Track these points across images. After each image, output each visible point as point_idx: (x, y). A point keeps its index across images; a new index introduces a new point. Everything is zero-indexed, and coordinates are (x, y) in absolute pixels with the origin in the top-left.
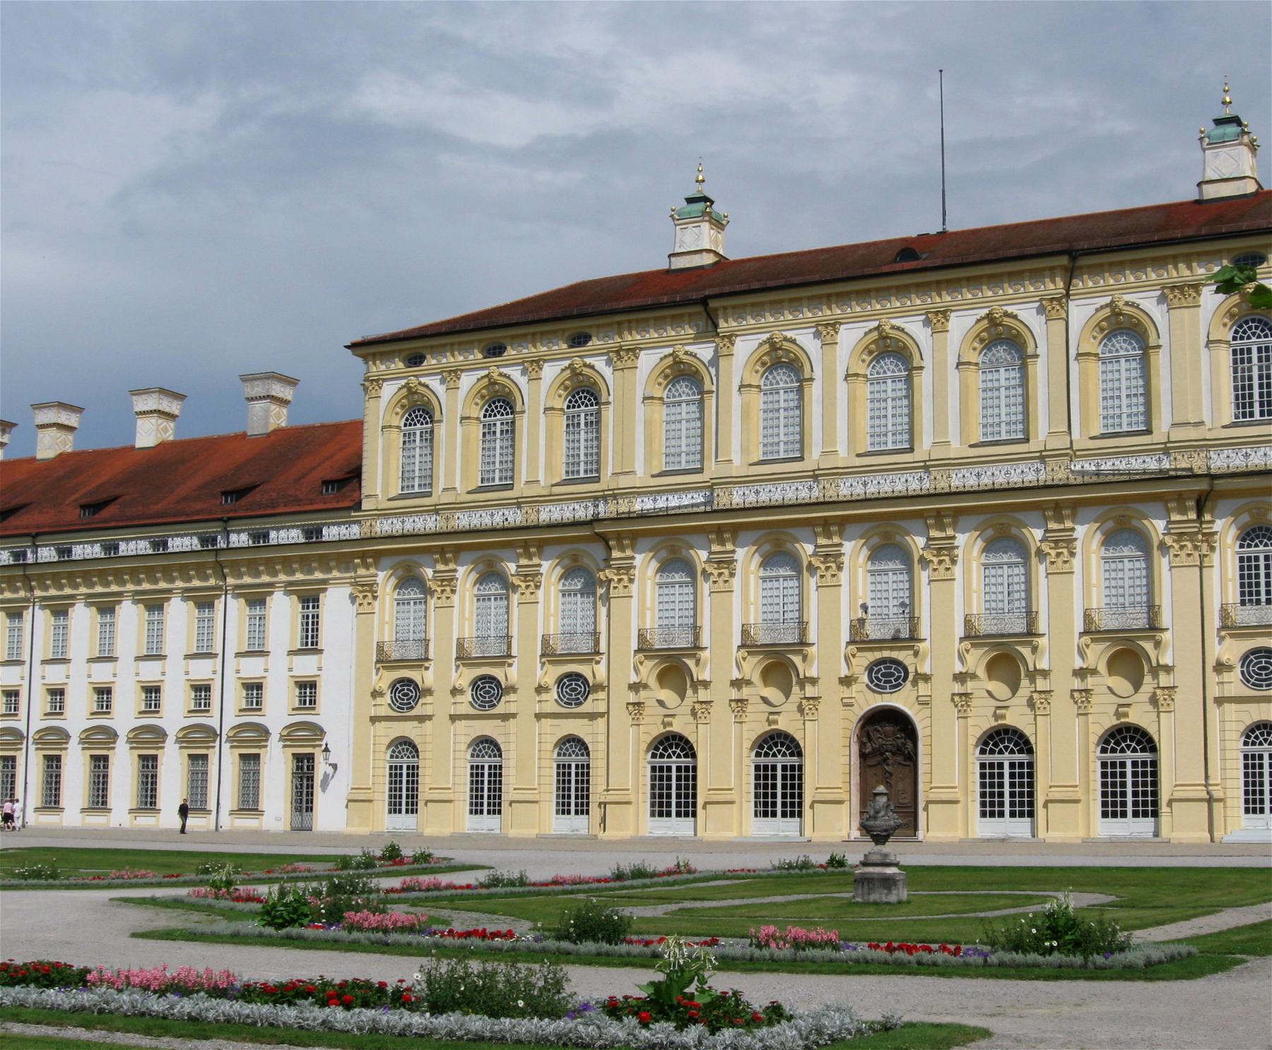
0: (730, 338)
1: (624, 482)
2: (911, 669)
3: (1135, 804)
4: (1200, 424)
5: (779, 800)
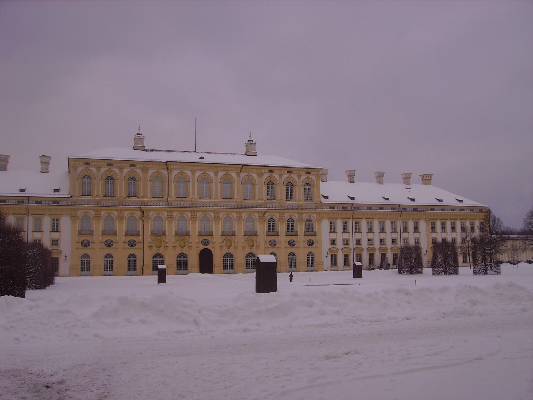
0: (172, 170)
1: (146, 199)
2: (211, 241)
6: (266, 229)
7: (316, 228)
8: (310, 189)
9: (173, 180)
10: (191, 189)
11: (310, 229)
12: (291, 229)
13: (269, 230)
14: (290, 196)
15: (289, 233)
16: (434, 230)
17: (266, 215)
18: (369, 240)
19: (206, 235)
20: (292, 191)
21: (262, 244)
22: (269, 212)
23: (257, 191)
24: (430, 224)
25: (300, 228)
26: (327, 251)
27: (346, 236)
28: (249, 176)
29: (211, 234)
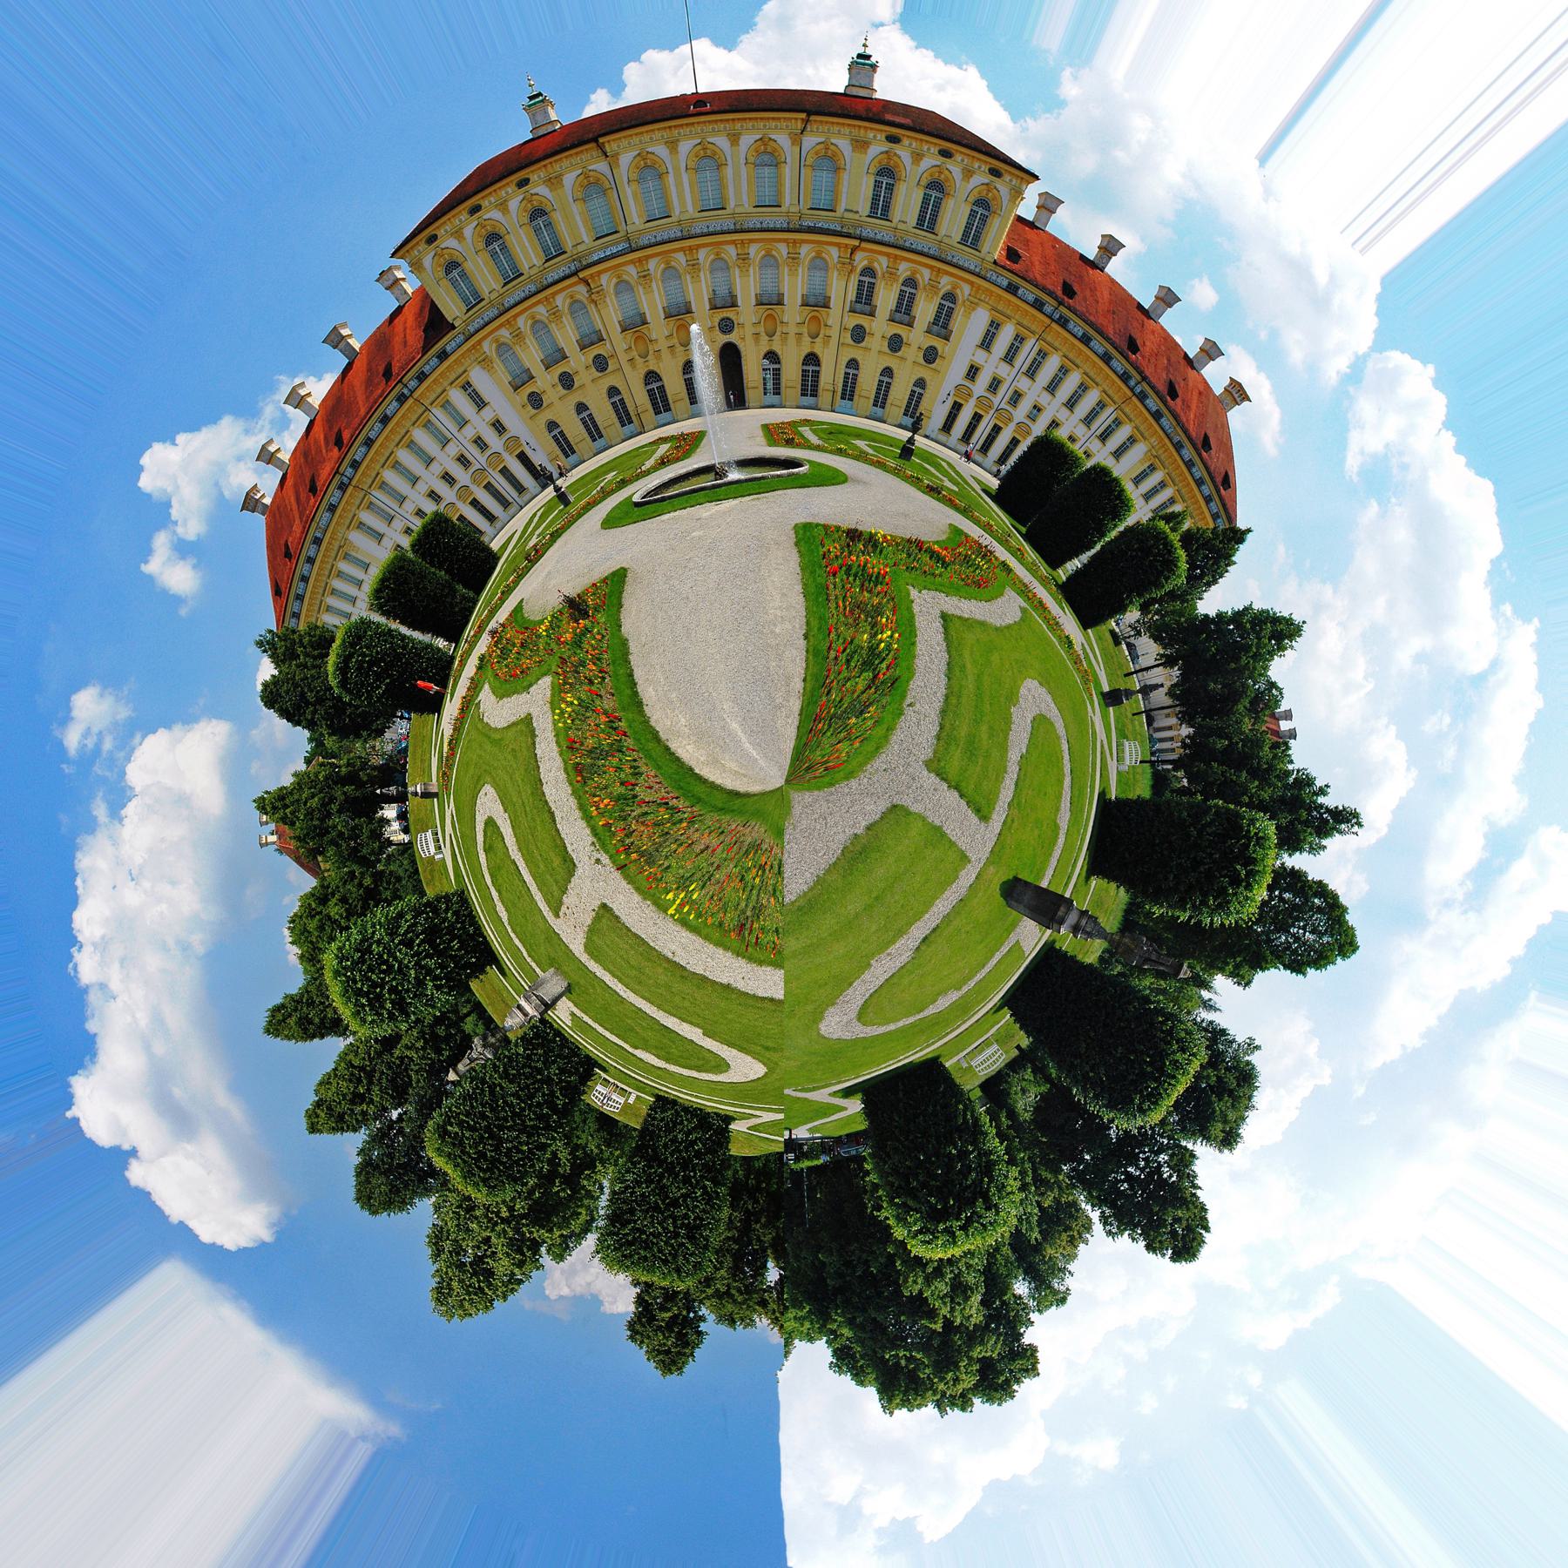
7: (956, 323)
11: (942, 324)
12: (904, 310)
14: (928, 219)
17: (859, 256)
20: (937, 205)
22: (865, 250)
23: (844, 189)
28: (826, 145)
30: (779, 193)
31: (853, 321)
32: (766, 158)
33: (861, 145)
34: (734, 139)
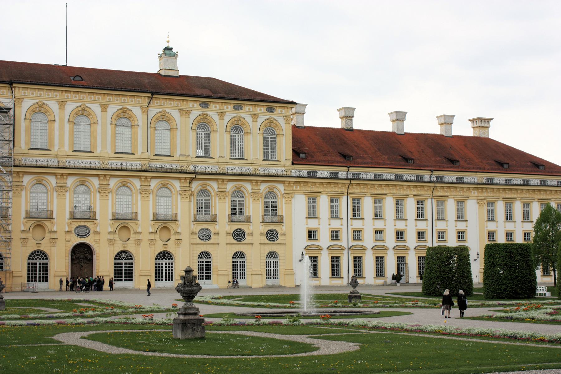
0: (21, 99)
3: (125, 277)
4: (189, 156)
5: (38, 276)
6: (193, 210)
7: (283, 208)
8: (274, 140)
9: (23, 117)
10: (56, 133)
13: (199, 209)
15: (235, 218)
16: (491, 217)
18: (376, 232)
19: (83, 220)
20: (241, 141)
21: (185, 237)
23: (178, 141)
24: (485, 207)
25: (254, 209)
26: (302, 250)
27: (336, 224)
29: (92, 218)
30: (134, 144)
31: (198, 227)
32: (124, 121)
33: (185, 113)
34: (104, 107)
